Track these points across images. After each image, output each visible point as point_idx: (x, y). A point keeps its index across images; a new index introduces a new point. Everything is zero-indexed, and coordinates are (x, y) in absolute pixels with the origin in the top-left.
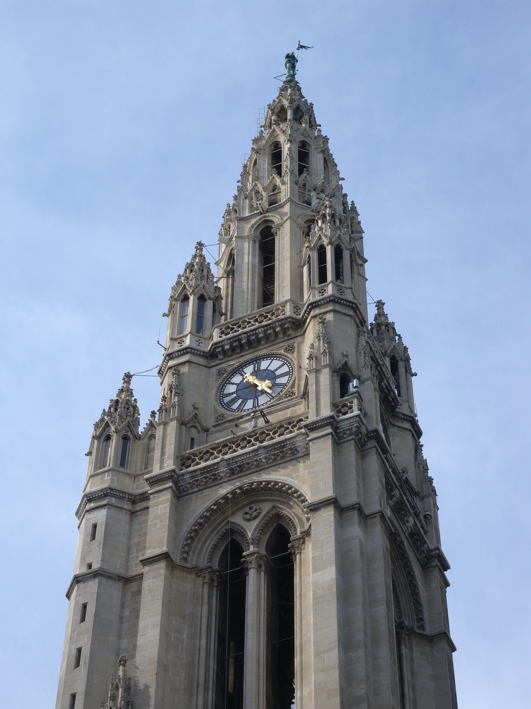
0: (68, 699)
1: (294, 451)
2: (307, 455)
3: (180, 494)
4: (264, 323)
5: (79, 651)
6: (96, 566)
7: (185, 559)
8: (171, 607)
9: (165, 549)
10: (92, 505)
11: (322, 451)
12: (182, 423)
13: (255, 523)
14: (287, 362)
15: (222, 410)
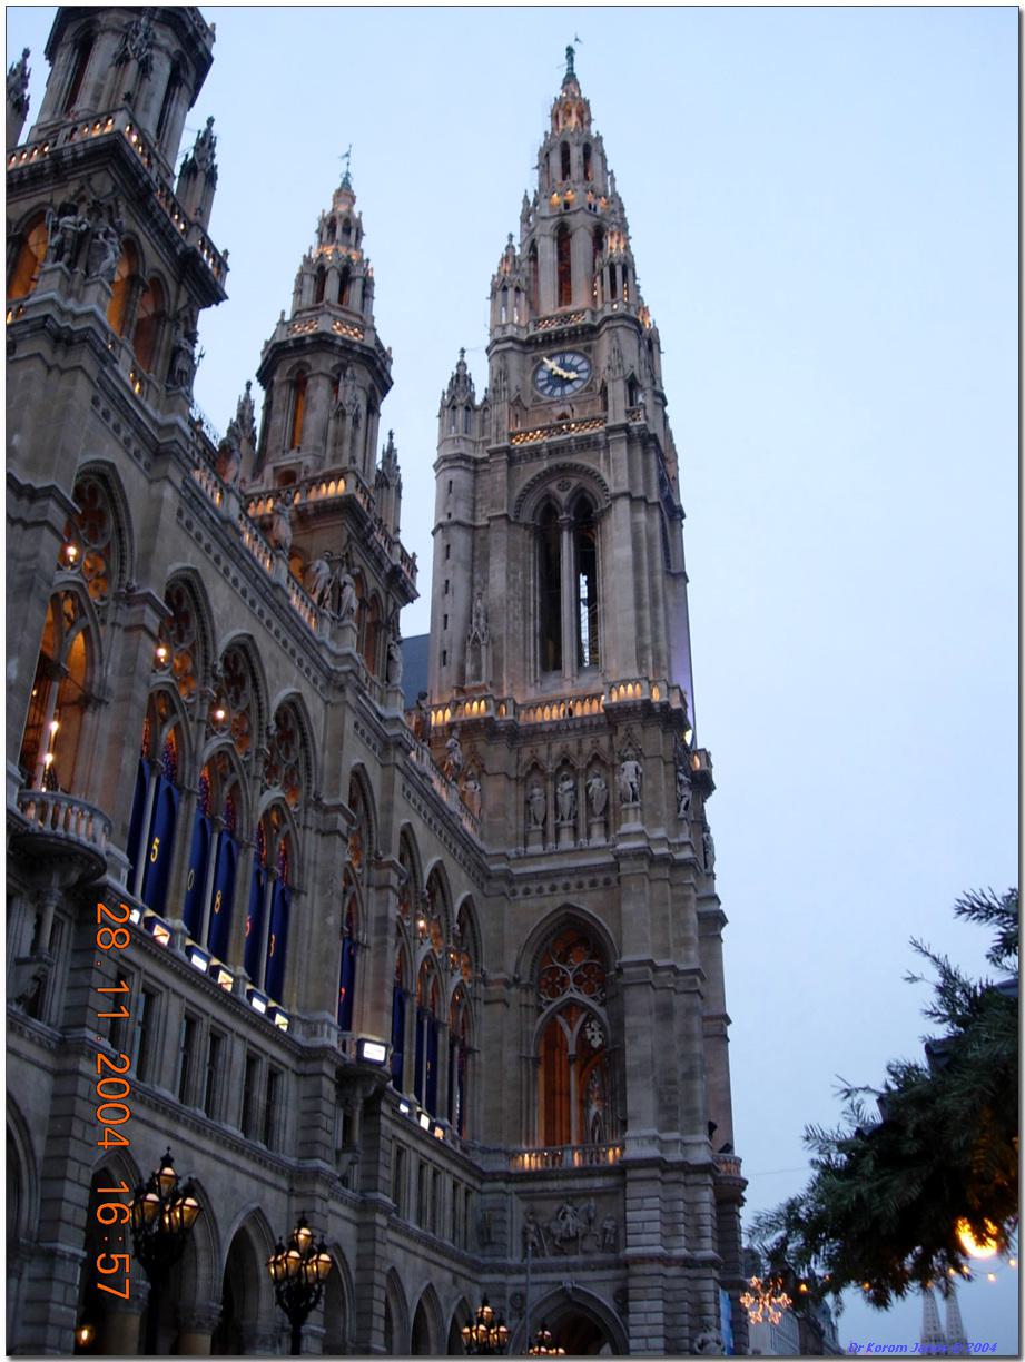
0: (440, 618)
1: (596, 443)
2: (607, 447)
3: (512, 461)
4: (569, 325)
5: (447, 582)
6: (453, 517)
7: (517, 517)
8: (512, 556)
9: (505, 511)
10: (447, 465)
11: (620, 451)
12: (511, 404)
13: (567, 493)
14: (586, 359)
15: (537, 393)
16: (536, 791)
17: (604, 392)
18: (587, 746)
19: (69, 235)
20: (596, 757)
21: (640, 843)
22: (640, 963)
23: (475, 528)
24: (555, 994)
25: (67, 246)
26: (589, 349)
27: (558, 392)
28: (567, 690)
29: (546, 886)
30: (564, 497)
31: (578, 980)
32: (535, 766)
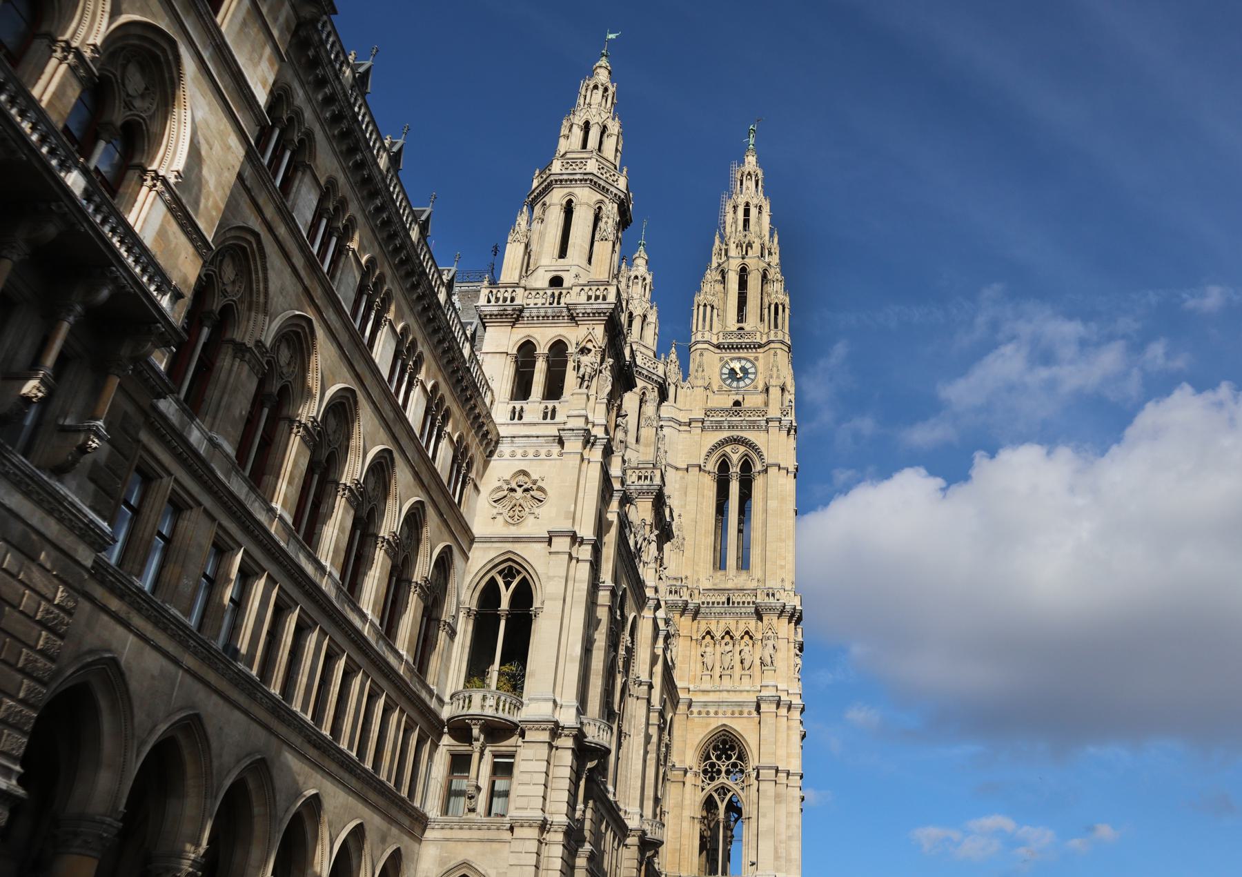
16: (710, 650)
17: (767, 390)
18: (742, 628)
19: (589, 370)
20: (747, 633)
21: (774, 693)
22: (770, 768)
23: (677, 469)
24: (712, 779)
25: (587, 378)
26: (756, 359)
27: (735, 384)
28: (730, 585)
29: (712, 711)
30: (735, 458)
31: (728, 772)
32: (708, 633)
